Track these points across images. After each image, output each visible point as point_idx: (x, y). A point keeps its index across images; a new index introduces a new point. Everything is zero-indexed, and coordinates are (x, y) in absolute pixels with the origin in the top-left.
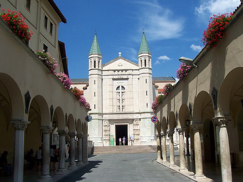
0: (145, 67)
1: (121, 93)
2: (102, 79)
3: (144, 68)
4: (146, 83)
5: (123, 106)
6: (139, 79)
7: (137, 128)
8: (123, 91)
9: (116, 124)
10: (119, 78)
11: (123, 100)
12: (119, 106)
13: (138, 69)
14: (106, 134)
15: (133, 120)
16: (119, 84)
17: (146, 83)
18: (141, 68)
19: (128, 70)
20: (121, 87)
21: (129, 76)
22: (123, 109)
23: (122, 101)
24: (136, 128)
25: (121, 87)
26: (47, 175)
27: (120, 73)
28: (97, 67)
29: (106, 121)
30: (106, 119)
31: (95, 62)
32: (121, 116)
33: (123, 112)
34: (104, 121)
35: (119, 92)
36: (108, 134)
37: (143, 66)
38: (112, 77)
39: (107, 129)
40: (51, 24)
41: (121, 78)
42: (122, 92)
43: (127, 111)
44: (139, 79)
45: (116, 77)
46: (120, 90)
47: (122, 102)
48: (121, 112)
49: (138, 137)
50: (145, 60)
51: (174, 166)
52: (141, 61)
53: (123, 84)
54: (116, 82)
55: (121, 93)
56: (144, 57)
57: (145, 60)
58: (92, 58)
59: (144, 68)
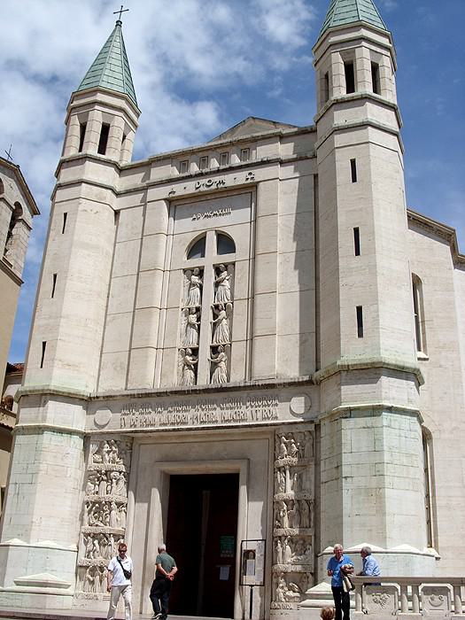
2: (117, 213)
4: (354, 180)
5: (214, 350)
8: (227, 258)
10: (202, 189)
11: (223, 313)
12: (195, 352)
14: (98, 530)
17: (354, 180)
19: (256, 141)
20: (211, 243)
21: (259, 174)
23: (215, 317)
25: (211, 243)
29: (106, 448)
30: (105, 430)
33: (213, 385)
34: (93, 448)
35: (201, 273)
36: (107, 529)
37: (340, 92)
38: (164, 192)
39: (103, 496)
41: (214, 187)
42: (218, 270)
44: (316, 176)
45: (190, 187)
47: (215, 324)
48: (203, 381)
50: (350, 70)
55: (210, 275)
57: (350, 70)
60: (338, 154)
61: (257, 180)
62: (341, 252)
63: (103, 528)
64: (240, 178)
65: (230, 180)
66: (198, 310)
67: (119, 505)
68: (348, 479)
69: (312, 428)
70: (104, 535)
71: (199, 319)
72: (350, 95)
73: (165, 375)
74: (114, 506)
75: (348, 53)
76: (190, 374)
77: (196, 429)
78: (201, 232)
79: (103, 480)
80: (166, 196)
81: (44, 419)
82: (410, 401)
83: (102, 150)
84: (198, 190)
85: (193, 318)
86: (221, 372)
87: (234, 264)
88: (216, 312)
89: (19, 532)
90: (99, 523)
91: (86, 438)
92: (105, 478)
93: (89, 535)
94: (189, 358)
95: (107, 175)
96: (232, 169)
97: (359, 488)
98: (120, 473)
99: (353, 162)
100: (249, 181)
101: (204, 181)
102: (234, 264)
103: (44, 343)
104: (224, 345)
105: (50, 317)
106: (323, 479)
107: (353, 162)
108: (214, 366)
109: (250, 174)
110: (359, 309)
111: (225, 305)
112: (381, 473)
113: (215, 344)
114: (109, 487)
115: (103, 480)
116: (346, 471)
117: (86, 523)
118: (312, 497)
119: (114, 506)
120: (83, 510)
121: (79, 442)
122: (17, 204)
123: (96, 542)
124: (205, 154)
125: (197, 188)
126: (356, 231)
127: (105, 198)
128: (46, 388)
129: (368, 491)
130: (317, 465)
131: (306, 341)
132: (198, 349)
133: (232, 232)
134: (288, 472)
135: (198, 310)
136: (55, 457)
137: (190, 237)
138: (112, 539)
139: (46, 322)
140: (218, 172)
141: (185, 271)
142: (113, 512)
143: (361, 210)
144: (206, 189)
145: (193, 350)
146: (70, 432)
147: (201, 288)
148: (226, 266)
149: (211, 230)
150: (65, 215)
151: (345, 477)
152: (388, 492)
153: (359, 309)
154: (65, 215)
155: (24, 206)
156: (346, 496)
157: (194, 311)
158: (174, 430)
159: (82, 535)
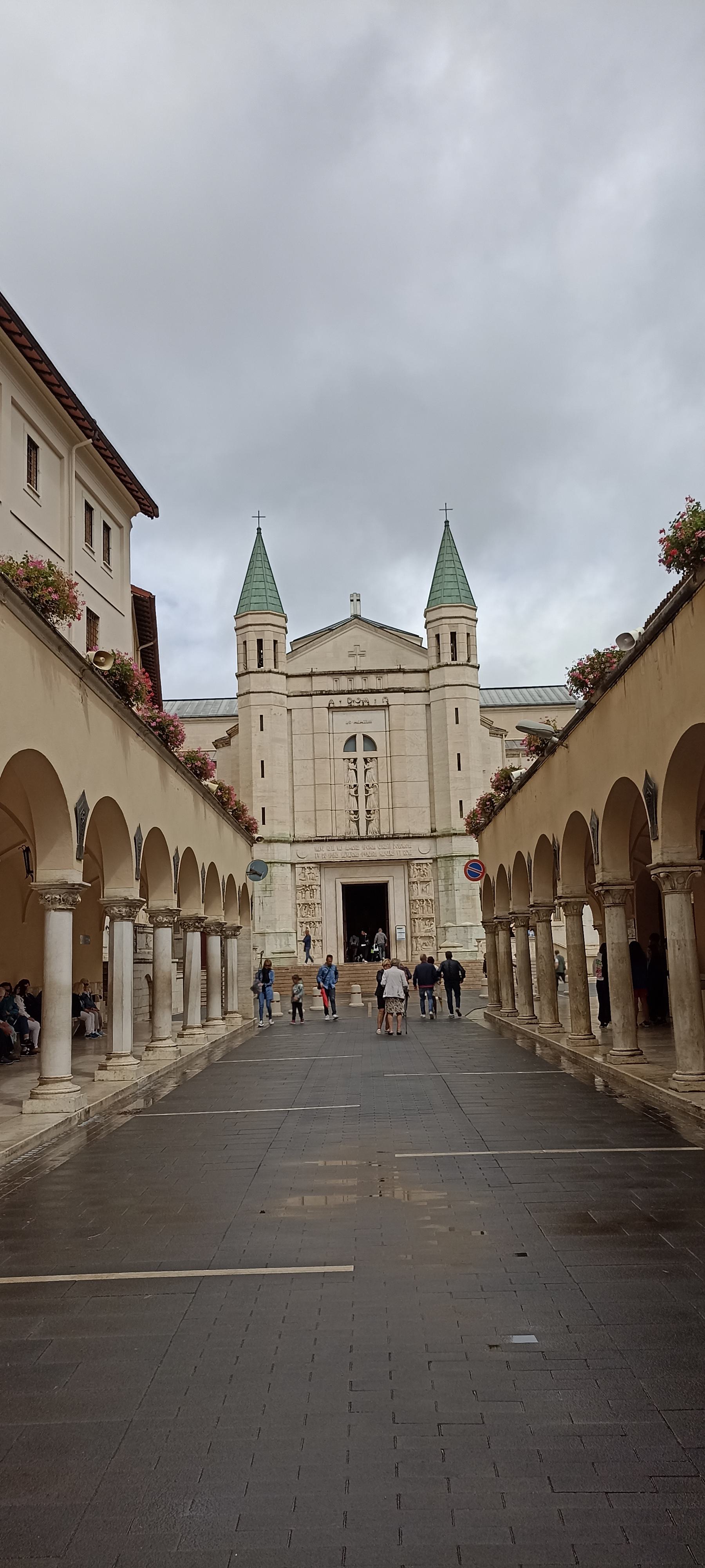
0: (455, 662)
1: (361, 763)
2: (289, 710)
3: (447, 665)
4: (457, 722)
5: (368, 812)
6: (428, 705)
7: (423, 896)
8: (370, 754)
11: (371, 791)
12: (356, 812)
13: (426, 668)
15: (407, 862)
16: (352, 730)
17: (457, 722)
18: (435, 664)
20: (360, 740)
21: (393, 698)
22: (370, 826)
23: (367, 791)
24: (419, 893)
25: (360, 740)
26: (168, 1038)
27: (359, 683)
28: (268, 664)
31: (260, 642)
34: (298, 869)
35: (355, 760)
36: (315, 919)
37: (447, 658)
40: (107, 528)
41: (361, 704)
42: (365, 760)
43: (385, 831)
44: (428, 705)
45: (343, 700)
46: (360, 753)
47: (366, 797)
48: (363, 833)
49: (427, 928)
50: (453, 635)
51: (530, 1021)
52: (438, 636)
53: (367, 729)
54: (340, 718)
55: (361, 763)
56: (447, 621)
57: (453, 635)
58: (250, 628)
59: (447, 665)
60: (448, 702)
62: (450, 767)
63: (310, 919)
65: (372, 699)
66: (355, 786)
67: (318, 904)
70: (313, 922)
71: (356, 792)
72: (455, 662)
73: (338, 827)
74: (316, 905)
75: (454, 626)
76: (354, 825)
78: (355, 734)
79: (307, 890)
85: (352, 791)
86: (373, 826)
88: (367, 788)
89: (269, 925)
90: (308, 916)
91: (293, 865)
93: (303, 923)
94: (353, 817)
95: (279, 683)
96: (372, 691)
97: (463, 895)
99: (457, 709)
101: (354, 697)
102: (377, 758)
103: (263, 809)
105: (265, 791)
106: (441, 888)
107: (457, 709)
108: (368, 822)
109: (385, 698)
110: (461, 802)
114: (312, 895)
115: (307, 890)
117: (299, 916)
118: (433, 898)
119: (316, 905)
120: (297, 909)
123: (308, 926)
128: (273, 839)
129: (468, 897)
130: (436, 880)
131: (424, 812)
132: (358, 811)
136: (281, 880)
138: (317, 924)
139: (260, 794)
141: (344, 759)
142: (317, 909)
143: (461, 742)
144: (356, 705)
145: (354, 811)
148: (371, 758)
153: (461, 802)
154: (261, 716)
156: (457, 898)
159: (298, 923)
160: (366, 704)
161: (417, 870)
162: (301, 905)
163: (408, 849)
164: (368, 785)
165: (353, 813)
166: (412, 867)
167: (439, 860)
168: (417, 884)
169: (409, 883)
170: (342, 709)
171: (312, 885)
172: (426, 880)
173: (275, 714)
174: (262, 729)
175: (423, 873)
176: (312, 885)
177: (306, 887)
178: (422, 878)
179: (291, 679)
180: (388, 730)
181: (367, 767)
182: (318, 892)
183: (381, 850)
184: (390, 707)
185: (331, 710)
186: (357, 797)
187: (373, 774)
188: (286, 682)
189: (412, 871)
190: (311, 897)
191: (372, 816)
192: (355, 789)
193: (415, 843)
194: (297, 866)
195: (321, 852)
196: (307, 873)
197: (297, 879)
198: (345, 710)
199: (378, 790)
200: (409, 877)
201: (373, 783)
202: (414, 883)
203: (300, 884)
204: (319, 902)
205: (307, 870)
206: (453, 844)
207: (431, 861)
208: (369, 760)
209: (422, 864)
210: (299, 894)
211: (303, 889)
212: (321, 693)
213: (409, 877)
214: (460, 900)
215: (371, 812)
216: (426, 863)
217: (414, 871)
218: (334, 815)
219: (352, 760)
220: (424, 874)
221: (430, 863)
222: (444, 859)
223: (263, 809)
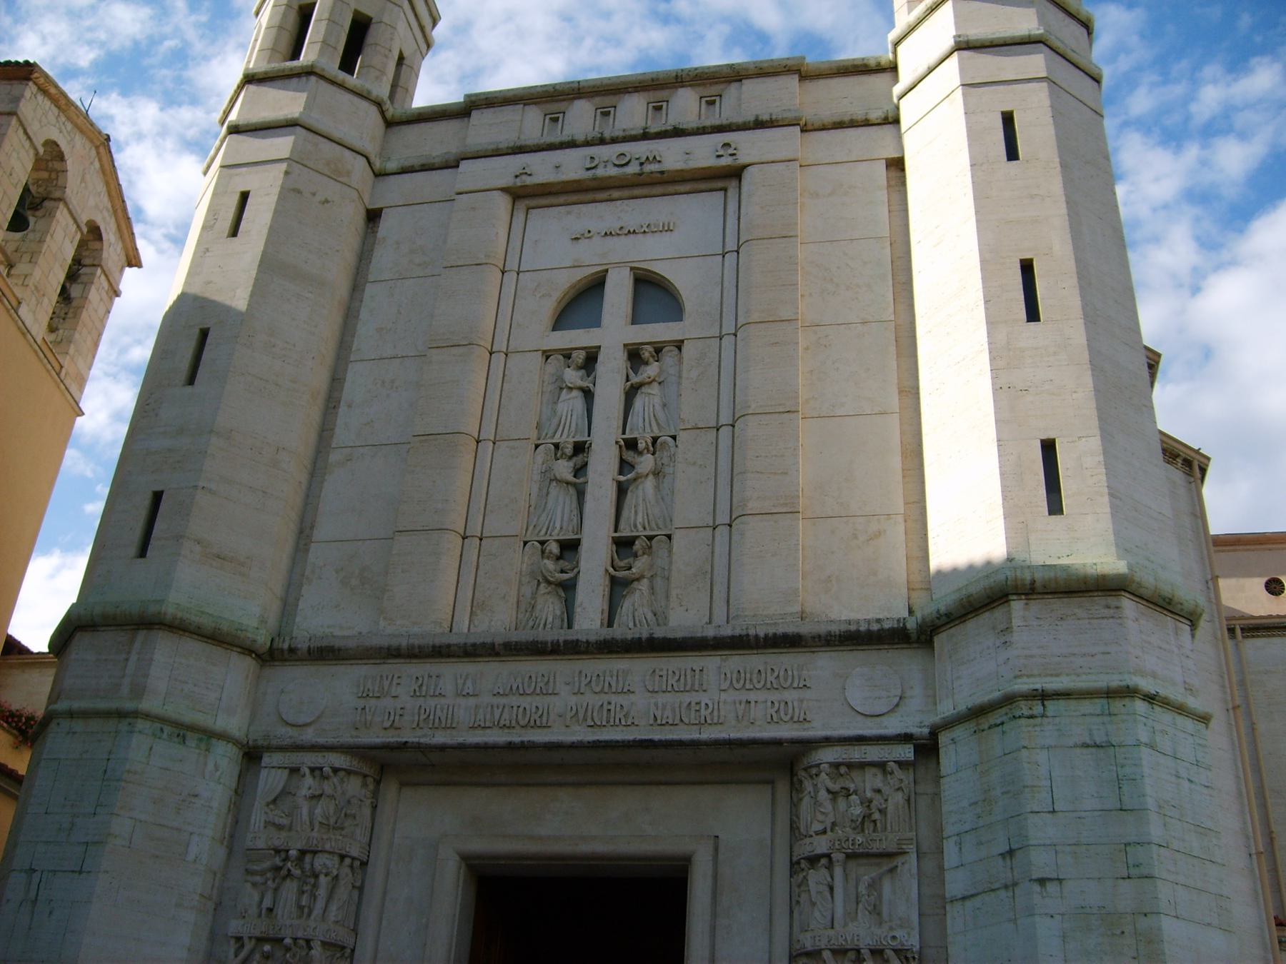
2: (373, 216)
4: (1012, 154)
5: (623, 545)
7: (863, 933)
9: (479, 845)
10: (600, 172)
11: (646, 463)
12: (570, 547)
16: (591, 256)
23: (624, 466)
29: (308, 784)
30: (309, 736)
32: (564, 700)
34: (270, 779)
35: (591, 359)
38: (504, 171)
39: (288, 923)
41: (633, 169)
42: (635, 356)
45: (572, 165)
47: (622, 490)
61: (743, 160)
64: (703, 153)
65: (673, 155)
68: (1051, 888)
69: (907, 752)
71: (580, 470)
77: (574, 746)
78: (600, 268)
79: (289, 874)
80: (507, 181)
81: (139, 691)
82: (1189, 689)
83: (347, 65)
84: (590, 174)
85: (564, 469)
87: (679, 345)
88: (629, 456)
91: (252, 755)
92: (297, 872)
98: (342, 857)
100: (726, 161)
102: (679, 345)
103: (157, 497)
104: (650, 538)
106: (956, 884)
108: (618, 586)
110: (1049, 448)
111: (655, 440)
112: (1145, 871)
113: (625, 532)
114: (305, 900)
115: (289, 874)
116: (1041, 862)
118: (913, 941)
121: (225, 759)
122: (95, 232)
124: (608, 100)
125: (588, 169)
126: (1027, 268)
127: (349, 173)
133: (680, 277)
134: (838, 871)
135: (580, 448)
137: (566, 281)
140: (646, 136)
141: (547, 355)
144: (613, 171)
146: (209, 735)
147: (588, 395)
148: (658, 350)
149: (619, 264)
150: (245, 196)
151: (1042, 881)
152: (1167, 924)
153: (1049, 448)
154: (245, 196)
155: (110, 234)
156: (1046, 929)
157: (569, 450)
158: (510, 746)
160: (649, 168)
161: (833, 794)
162: (249, 946)
163: (790, 695)
164: (631, 444)
165: (554, 548)
166: (808, 785)
167: (943, 739)
168: (830, 867)
169: (794, 866)
170: (562, 199)
171: (315, 853)
172: (876, 847)
173: (299, 192)
174: (234, 232)
175: (857, 811)
176: (315, 853)
177: (286, 859)
178: (860, 839)
179: (396, 129)
180: (731, 245)
181: (635, 379)
182: (343, 892)
183: (661, 699)
184: (747, 175)
185: (522, 205)
186: (581, 494)
187: (657, 401)
188: (386, 132)
189: (806, 802)
190: (301, 908)
191: (640, 565)
192: (579, 459)
193: (824, 664)
194: (266, 760)
195: (387, 703)
196: (304, 792)
197: (258, 816)
198: (575, 198)
199: (672, 458)
200: (795, 831)
201: (656, 433)
202: (813, 860)
203: (261, 844)
204: (342, 936)
205: (309, 780)
206: (1018, 637)
207: (907, 752)
208: (647, 353)
209: (862, 766)
210: (250, 897)
211: (277, 869)
212: (497, 153)
213: (795, 831)
214: (1064, 937)
215: (638, 545)
216: (881, 766)
217: (817, 803)
218: (472, 555)
219: (579, 357)
220: (866, 817)
221: (902, 764)
222: (971, 725)
223: (157, 497)
